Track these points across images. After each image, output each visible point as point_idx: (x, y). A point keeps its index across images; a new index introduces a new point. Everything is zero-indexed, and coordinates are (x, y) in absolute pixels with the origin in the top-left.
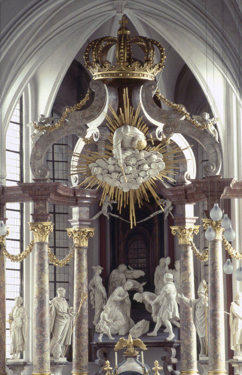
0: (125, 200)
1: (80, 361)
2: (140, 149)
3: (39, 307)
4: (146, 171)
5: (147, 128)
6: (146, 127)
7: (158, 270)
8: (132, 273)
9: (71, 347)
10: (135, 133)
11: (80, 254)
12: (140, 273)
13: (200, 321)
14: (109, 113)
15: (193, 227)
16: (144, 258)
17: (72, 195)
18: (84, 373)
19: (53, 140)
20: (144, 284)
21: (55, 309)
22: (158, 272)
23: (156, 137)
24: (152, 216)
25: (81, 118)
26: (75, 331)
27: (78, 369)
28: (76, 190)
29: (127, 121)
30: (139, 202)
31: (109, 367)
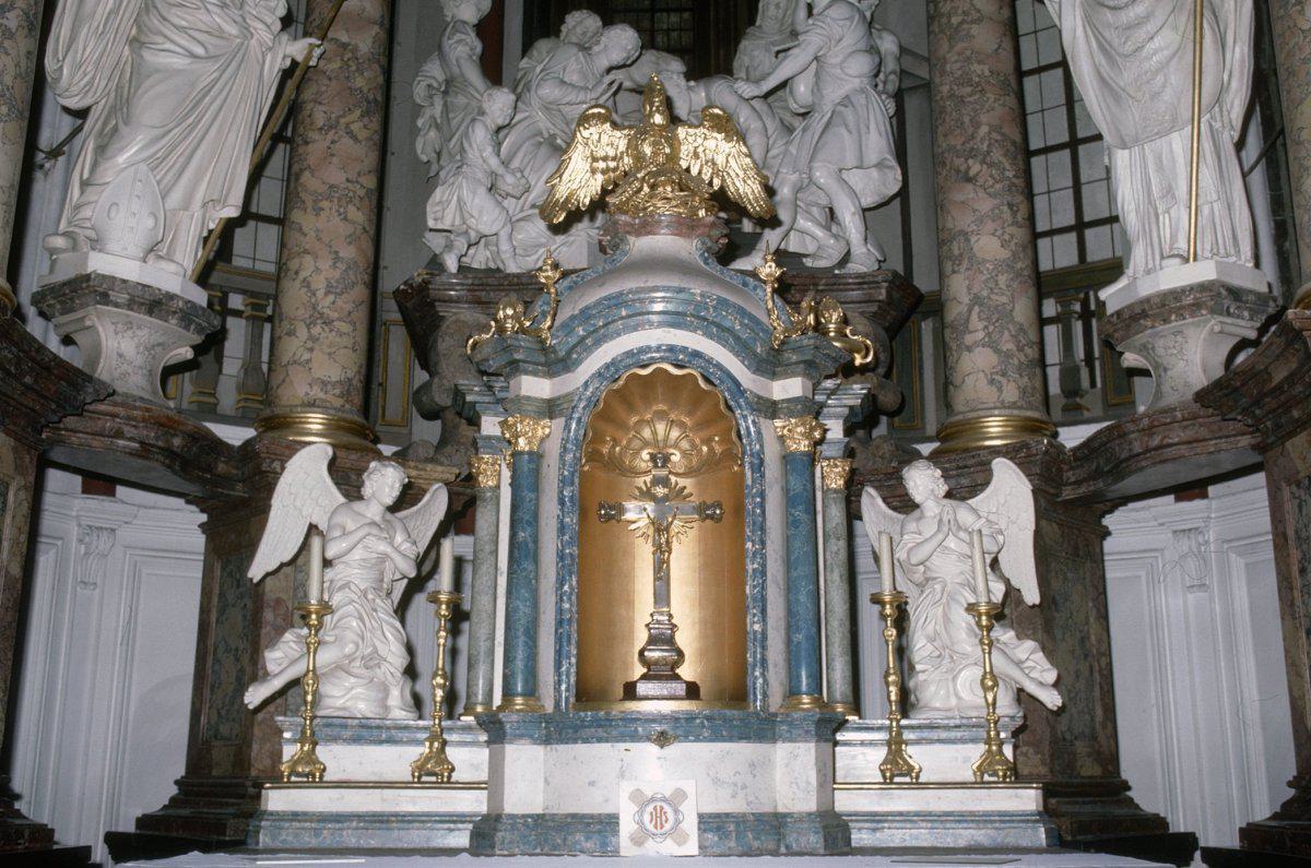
1: (311, 350)
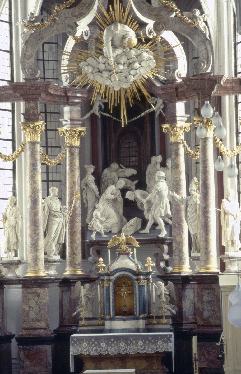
0: (116, 98)
1: (74, 259)
2: (130, 47)
3: (33, 206)
4: (137, 70)
5: (138, 26)
6: (136, 24)
7: (150, 168)
8: (124, 171)
9: (64, 246)
10: (125, 30)
11: (72, 154)
12: (132, 172)
13: (192, 218)
14: (99, 11)
15: (184, 125)
16: (135, 156)
17: (63, 94)
18: (78, 271)
19: (43, 39)
20: (136, 182)
21: (48, 207)
22: (150, 170)
23: (146, 35)
24: (143, 114)
25: (71, 16)
26: (69, 230)
27: (71, 267)
28: (67, 90)
29: (117, 18)
30: (130, 100)
31: (103, 264)
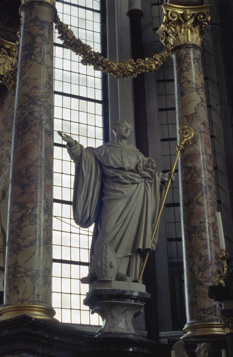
1: (196, 297)
18: (213, 326)
